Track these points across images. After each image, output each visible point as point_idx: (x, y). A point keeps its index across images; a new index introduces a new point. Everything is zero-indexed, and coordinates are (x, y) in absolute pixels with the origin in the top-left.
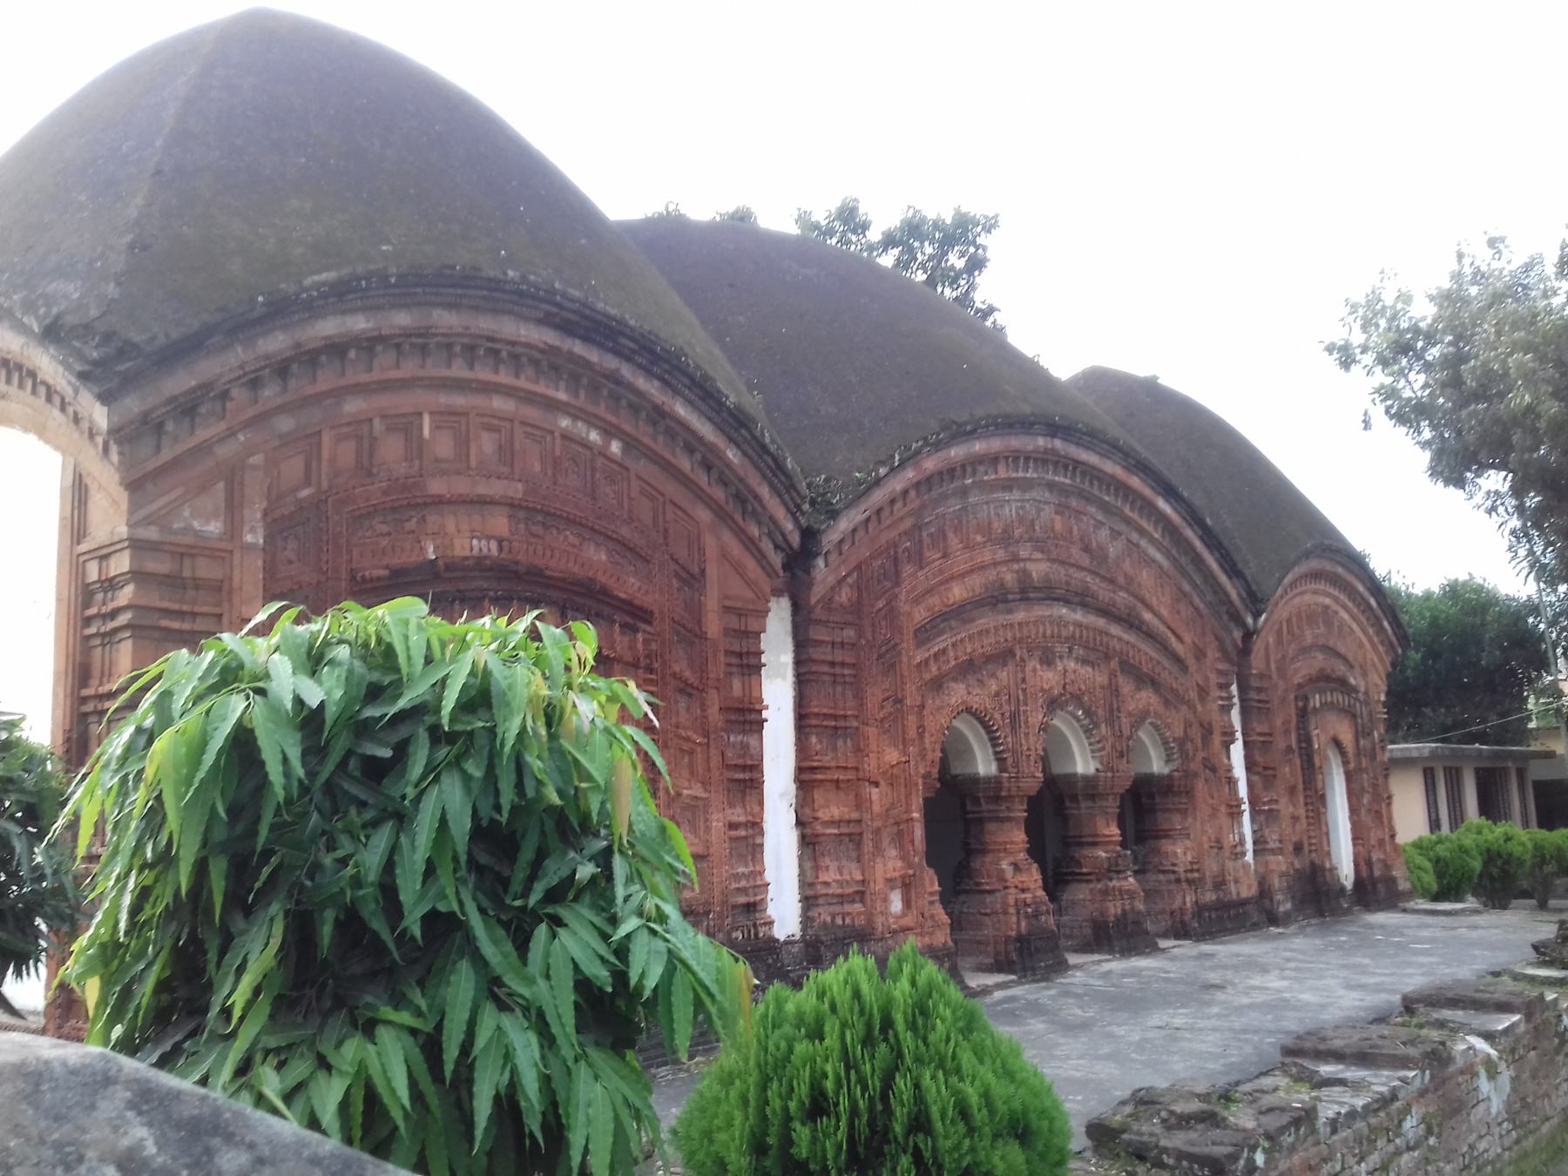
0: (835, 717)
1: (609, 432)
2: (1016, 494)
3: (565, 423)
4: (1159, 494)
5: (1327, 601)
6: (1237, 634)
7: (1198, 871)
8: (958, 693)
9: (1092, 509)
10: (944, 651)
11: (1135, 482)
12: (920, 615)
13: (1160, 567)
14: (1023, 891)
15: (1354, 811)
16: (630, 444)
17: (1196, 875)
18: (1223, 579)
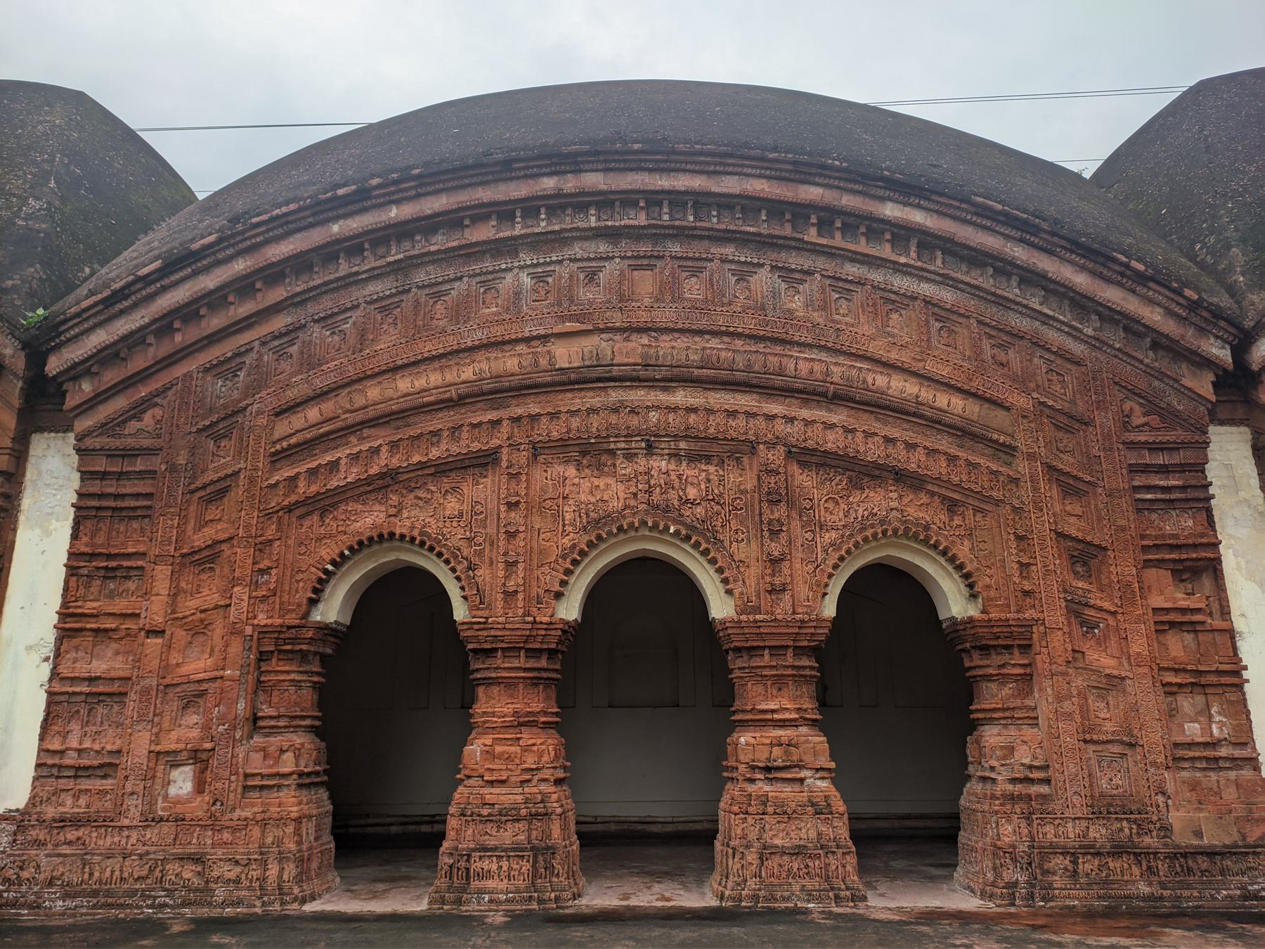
0: (110, 557)
2: (526, 258)
4: (882, 199)
6: (1204, 385)
7: (1047, 781)
9: (729, 250)
10: (334, 466)
11: (812, 193)
12: (282, 428)
13: (927, 302)
14: (491, 783)
17: (1044, 789)
18: (1112, 295)
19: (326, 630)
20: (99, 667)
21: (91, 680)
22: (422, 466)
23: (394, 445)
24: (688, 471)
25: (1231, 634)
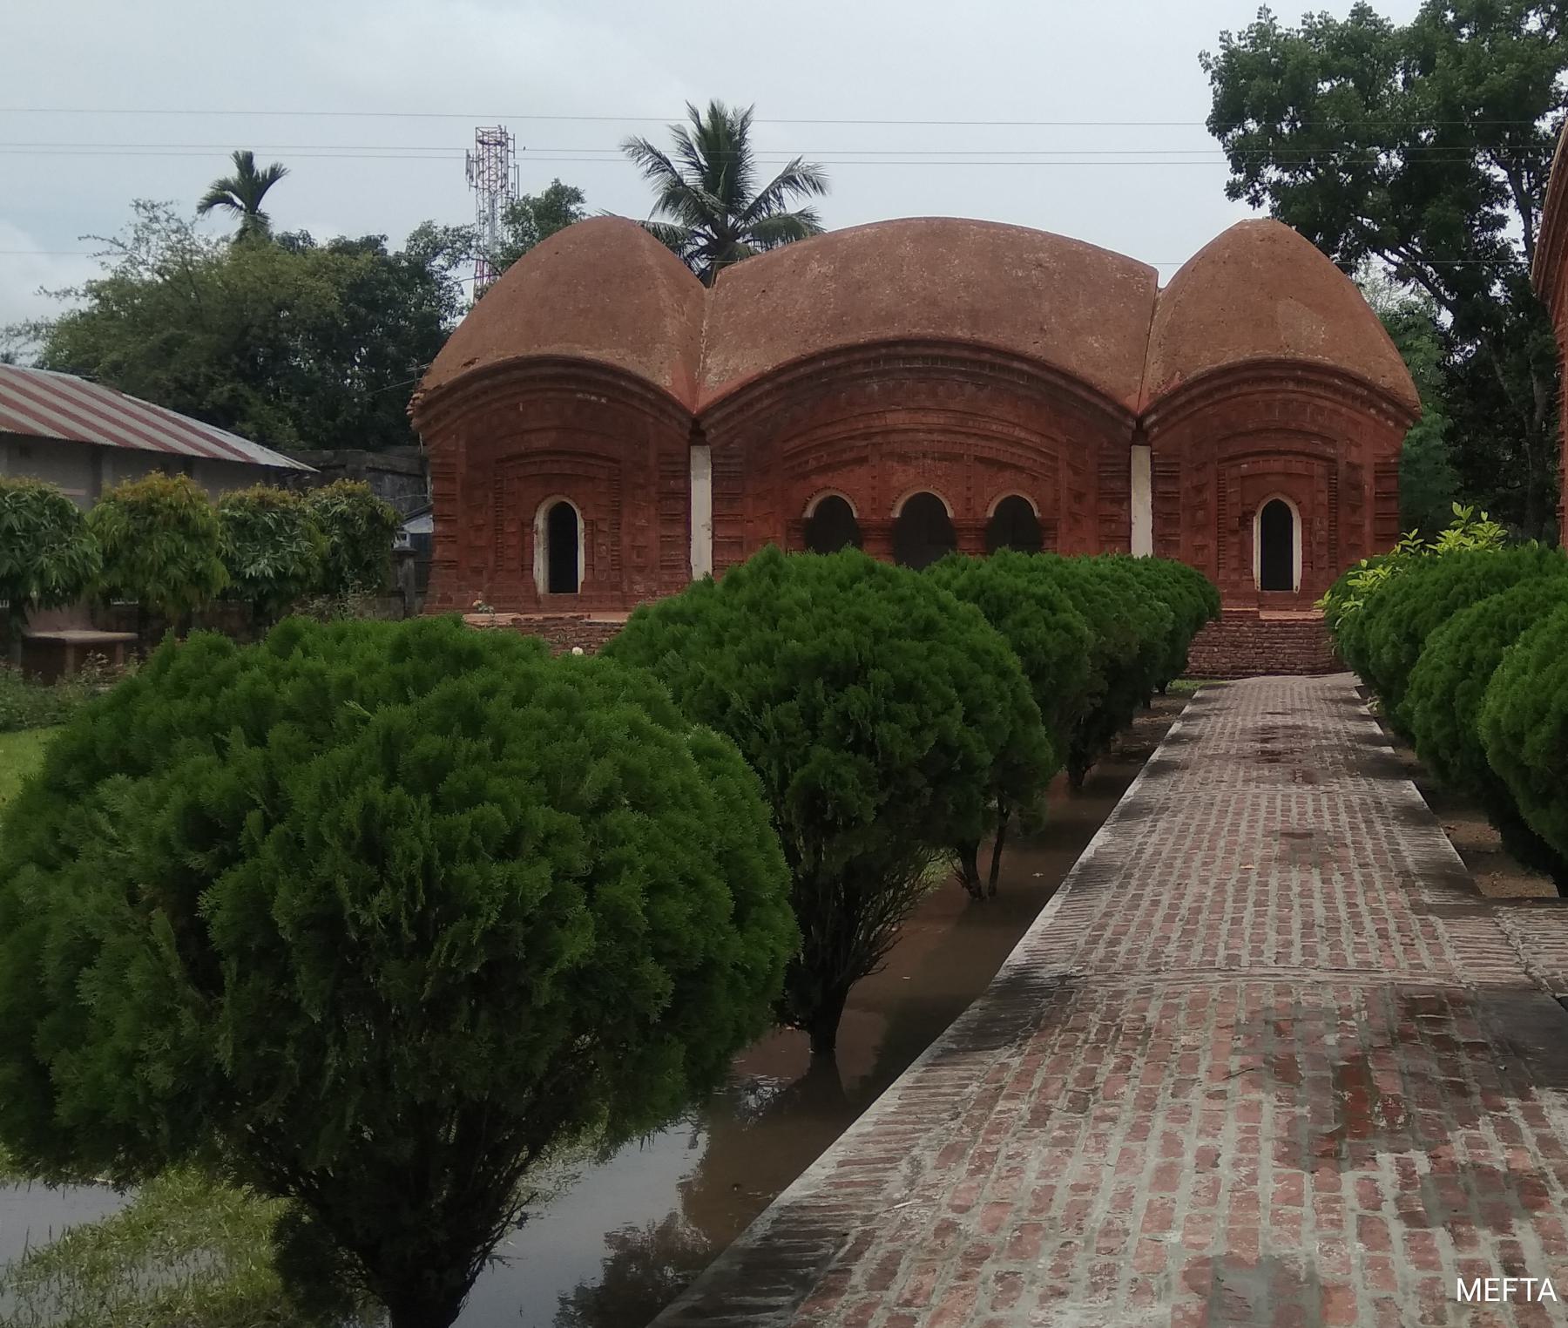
1: (600, 396)
3: (579, 396)
5: (1293, 396)
8: (819, 481)
15: (1306, 544)
16: (609, 399)
19: (807, 519)
20: (731, 533)
21: (729, 538)
22: (839, 462)
23: (829, 455)
24: (938, 464)
25: (1130, 523)
